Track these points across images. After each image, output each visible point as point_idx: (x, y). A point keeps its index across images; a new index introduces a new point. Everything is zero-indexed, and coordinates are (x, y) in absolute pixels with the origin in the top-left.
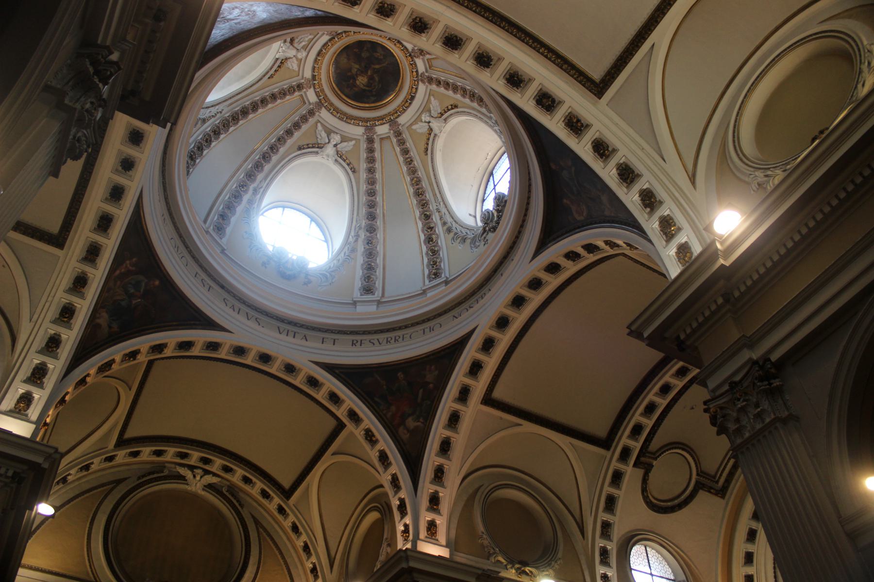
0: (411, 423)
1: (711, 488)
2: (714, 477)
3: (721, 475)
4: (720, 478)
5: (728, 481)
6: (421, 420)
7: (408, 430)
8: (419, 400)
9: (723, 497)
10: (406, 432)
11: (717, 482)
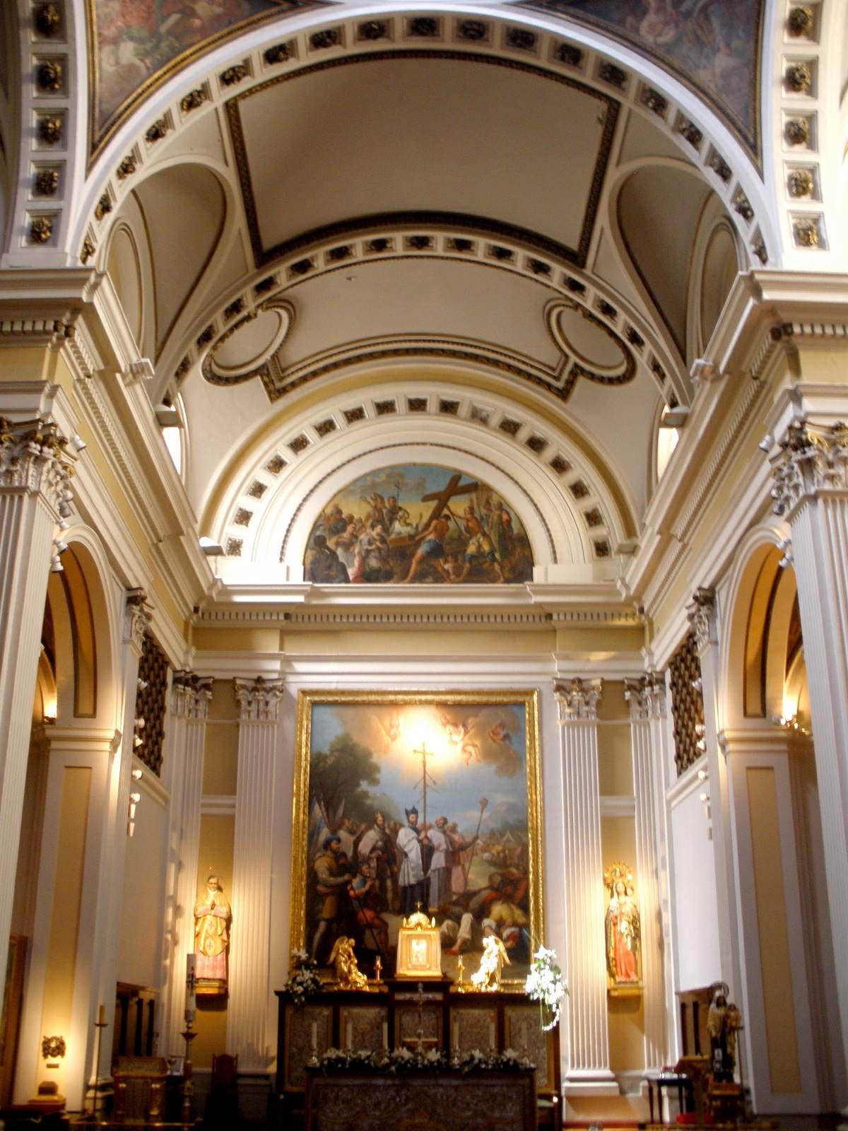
0: (128, 51)
1: (272, 382)
2: (283, 371)
3: (293, 373)
4: (289, 375)
5: (294, 385)
6: (148, 61)
7: (117, 63)
8: (163, 28)
9: (272, 400)
10: (112, 61)
11: (282, 379)
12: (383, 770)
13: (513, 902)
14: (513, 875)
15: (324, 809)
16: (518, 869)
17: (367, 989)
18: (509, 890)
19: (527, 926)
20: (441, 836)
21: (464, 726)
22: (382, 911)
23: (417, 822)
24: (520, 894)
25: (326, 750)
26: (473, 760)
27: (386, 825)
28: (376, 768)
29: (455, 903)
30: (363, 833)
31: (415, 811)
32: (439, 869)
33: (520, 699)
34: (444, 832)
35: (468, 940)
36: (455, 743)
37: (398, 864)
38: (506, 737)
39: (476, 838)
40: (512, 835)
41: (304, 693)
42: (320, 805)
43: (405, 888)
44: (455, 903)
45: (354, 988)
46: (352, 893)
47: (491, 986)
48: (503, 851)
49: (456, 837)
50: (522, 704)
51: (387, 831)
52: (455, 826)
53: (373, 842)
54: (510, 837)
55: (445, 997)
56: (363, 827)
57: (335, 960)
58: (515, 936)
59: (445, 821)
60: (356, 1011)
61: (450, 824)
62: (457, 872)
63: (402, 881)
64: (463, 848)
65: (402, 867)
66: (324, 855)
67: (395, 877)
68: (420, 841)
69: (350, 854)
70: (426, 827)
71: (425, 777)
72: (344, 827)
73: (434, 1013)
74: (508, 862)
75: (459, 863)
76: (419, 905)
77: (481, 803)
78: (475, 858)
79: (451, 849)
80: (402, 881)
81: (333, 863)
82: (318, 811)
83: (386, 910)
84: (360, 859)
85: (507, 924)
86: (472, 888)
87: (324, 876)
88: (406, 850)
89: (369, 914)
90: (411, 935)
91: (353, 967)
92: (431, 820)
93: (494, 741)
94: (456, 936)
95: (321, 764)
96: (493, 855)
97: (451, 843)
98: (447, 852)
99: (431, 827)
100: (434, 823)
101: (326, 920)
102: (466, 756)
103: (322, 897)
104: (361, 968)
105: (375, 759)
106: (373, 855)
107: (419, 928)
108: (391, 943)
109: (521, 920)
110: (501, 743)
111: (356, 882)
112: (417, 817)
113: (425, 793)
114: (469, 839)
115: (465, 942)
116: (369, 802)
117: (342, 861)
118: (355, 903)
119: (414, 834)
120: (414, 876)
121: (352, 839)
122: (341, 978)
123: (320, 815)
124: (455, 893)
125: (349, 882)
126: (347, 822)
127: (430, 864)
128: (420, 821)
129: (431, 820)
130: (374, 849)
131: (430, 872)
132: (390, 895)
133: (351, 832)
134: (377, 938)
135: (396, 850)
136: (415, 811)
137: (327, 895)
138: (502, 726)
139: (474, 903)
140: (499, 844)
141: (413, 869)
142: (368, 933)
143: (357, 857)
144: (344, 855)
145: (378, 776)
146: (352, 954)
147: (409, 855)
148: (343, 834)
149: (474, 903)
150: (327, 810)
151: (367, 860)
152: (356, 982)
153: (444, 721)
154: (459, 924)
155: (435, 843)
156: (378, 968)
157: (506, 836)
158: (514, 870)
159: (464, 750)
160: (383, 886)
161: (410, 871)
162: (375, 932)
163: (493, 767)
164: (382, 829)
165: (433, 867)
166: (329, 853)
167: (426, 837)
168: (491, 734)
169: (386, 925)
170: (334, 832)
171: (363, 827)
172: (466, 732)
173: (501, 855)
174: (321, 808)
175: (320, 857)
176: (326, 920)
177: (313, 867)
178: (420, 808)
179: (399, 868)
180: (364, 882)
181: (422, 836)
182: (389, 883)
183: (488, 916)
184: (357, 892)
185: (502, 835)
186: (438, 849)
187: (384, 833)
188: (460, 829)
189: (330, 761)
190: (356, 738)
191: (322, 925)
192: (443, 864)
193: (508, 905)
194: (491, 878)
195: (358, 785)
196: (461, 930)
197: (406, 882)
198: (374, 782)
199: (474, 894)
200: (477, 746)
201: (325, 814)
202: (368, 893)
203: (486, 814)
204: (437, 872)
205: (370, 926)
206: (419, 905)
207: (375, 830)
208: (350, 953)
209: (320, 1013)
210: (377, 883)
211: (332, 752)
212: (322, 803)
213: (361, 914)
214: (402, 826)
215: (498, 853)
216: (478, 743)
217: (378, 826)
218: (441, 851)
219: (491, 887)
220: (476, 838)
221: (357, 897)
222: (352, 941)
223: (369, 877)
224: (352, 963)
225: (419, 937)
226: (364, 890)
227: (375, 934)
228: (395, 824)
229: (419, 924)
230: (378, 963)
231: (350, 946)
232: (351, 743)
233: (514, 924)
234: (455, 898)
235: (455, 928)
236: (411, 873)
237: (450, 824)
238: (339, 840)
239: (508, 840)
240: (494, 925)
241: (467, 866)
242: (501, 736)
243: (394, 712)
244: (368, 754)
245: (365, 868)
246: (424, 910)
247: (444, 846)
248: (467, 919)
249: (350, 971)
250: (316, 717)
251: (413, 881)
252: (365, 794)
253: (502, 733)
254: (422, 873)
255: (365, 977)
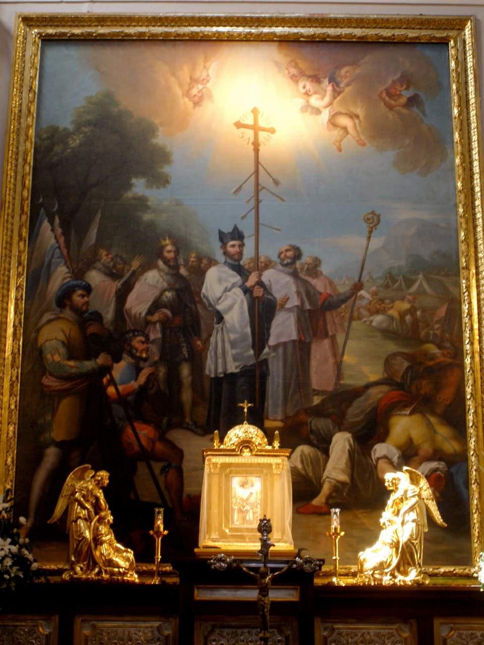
12: (176, 156)
13: (433, 413)
14: (433, 357)
15: (59, 231)
16: (440, 347)
17: (134, 578)
18: (426, 386)
19: (462, 458)
20: (288, 279)
21: (332, 80)
22: (171, 426)
23: (241, 254)
24: (446, 395)
25: (66, 123)
26: (350, 142)
27: (181, 261)
28: (164, 156)
29: (318, 412)
30: (135, 276)
31: (237, 235)
32: (285, 344)
33: (439, 34)
34: (295, 275)
35: (343, 484)
36: (317, 111)
37: (204, 335)
38: (413, 101)
39: (358, 286)
40: (428, 280)
41: (28, 21)
42: (52, 222)
43: (217, 381)
44: (318, 412)
45: (105, 576)
46: (111, 390)
47: (405, 573)
48: (412, 311)
49: (318, 284)
50: (443, 43)
51: (183, 271)
52: (317, 262)
53: (156, 293)
54: (426, 286)
55: (302, 595)
56: (136, 264)
57: (66, 512)
58: (439, 477)
59: (298, 254)
60: (110, 625)
61: (306, 259)
62: (320, 351)
63: (212, 367)
64: (331, 304)
65: (212, 339)
66: (58, 318)
67: (197, 360)
68: (247, 291)
69: (109, 315)
70: (261, 266)
71: (257, 172)
72: (99, 265)
73: (281, 632)
74: (423, 334)
75: (326, 335)
76: (246, 406)
77: (367, 220)
78: (355, 324)
79: (308, 306)
80: (212, 367)
81: (75, 332)
82: (49, 234)
83: (181, 426)
84: (130, 326)
85: (422, 453)
86: (349, 381)
87: (57, 358)
88: (220, 307)
89: (145, 432)
90: (230, 465)
91: (103, 529)
92: (269, 251)
93: (391, 108)
94: (319, 478)
95: (58, 149)
96: (392, 318)
97: (308, 294)
98: (300, 309)
99: (268, 265)
100: (274, 258)
101: (60, 445)
102: (336, 133)
103: (51, 398)
104: (122, 534)
105: (160, 139)
106: (156, 317)
107: (246, 453)
108: (188, 489)
109: (451, 447)
110: (404, 111)
111: (120, 369)
112: (242, 245)
113: (258, 201)
114: (343, 288)
115: (338, 488)
116: (147, 217)
117: (92, 329)
118: (119, 411)
119: (237, 279)
120: (235, 359)
121: (114, 286)
122: (78, 553)
123: (53, 241)
124: (317, 393)
125: (107, 369)
126: (103, 253)
127: (269, 335)
128: (248, 252)
129: (269, 251)
130: (156, 306)
131: (266, 350)
132: (187, 396)
133: (113, 274)
134: (161, 479)
135: (199, 307)
136: (237, 235)
137: (63, 394)
138: (407, 80)
139: (356, 411)
140: (403, 299)
141: (233, 344)
142: (142, 469)
143: (124, 321)
144: (97, 317)
145: (166, 169)
146: (102, 501)
147: (227, 317)
148: (95, 277)
149: (356, 411)
150: (66, 233)
151: (143, 327)
152: (110, 563)
153: (293, 71)
154: (326, 452)
155: (278, 295)
156: (158, 533)
157: (418, 283)
158: (433, 349)
159: (332, 123)
160: (173, 376)
161: (228, 346)
162: (157, 467)
163: (391, 154)
164: (173, 267)
165: (272, 342)
166: (68, 313)
167: (260, 283)
168: (384, 95)
169: (180, 454)
170: (79, 273)
171: (136, 264)
172: (336, 93)
173: (408, 318)
174: (53, 230)
175: (50, 321)
176: (60, 445)
177: (36, 339)
178: (247, 228)
179: (207, 341)
180: (138, 370)
181: (252, 280)
182: (185, 371)
183: (383, 437)
184: (120, 388)
185: (409, 283)
186: (282, 306)
187: (178, 276)
188: (325, 269)
189: (75, 142)
190: (126, 101)
191: (51, 455)
192: (294, 336)
193: (424, 416)
194: (388, 362)
195: (129, 186)
196: (329, 465)
197: (220, 370)
198: (161, 181)
199: (357, 393)
200: (357, 117)
201: (62, 239)
202: (143, 389)
203: (376, 242)
204: (281, 350)
205: (147, 456)
206: (246, 406)
207: (160, 270)
208: (97, 499)
209: (31, 632)
210: (162, 371)
211: (79, 126)
212: (57, 220)
213: (129, 431)
214: (212, 262)
215: (402, 315)
216: (359, 111)
217: (166, 262)
218: (290, 310)
219: (387, 381)
220: (358, 286)
221: (122, 399)
222: (104, 475)
223: (145, 360)
224: (101, 520)
225: (246, 470)
226: (135, 385)
227: (157, 471)
228: (199, 259)
229: (246, 444)
230: (160, 523)
231: (99, 484)
232: (115, 110)
233: (438, 454)
234: (316, 400)
235: (318, 460)
236: (230, 352)
237: (306, 259)
238: (88, 289)
239: (421, 292)
240: (395, 455)
241: (340, 339)
242: (403, 100)
243: (198, 53)
244: (149, 130)
245: (137, 342)
246: (257, 419)
247: (294, 301)
248: (341, 443)
249: (97, 541)
250: (48, 63)
251: (233, 368)
252: (142, 203)
253: (407, 94)
254: (252, 352)
255: (131, 555)
